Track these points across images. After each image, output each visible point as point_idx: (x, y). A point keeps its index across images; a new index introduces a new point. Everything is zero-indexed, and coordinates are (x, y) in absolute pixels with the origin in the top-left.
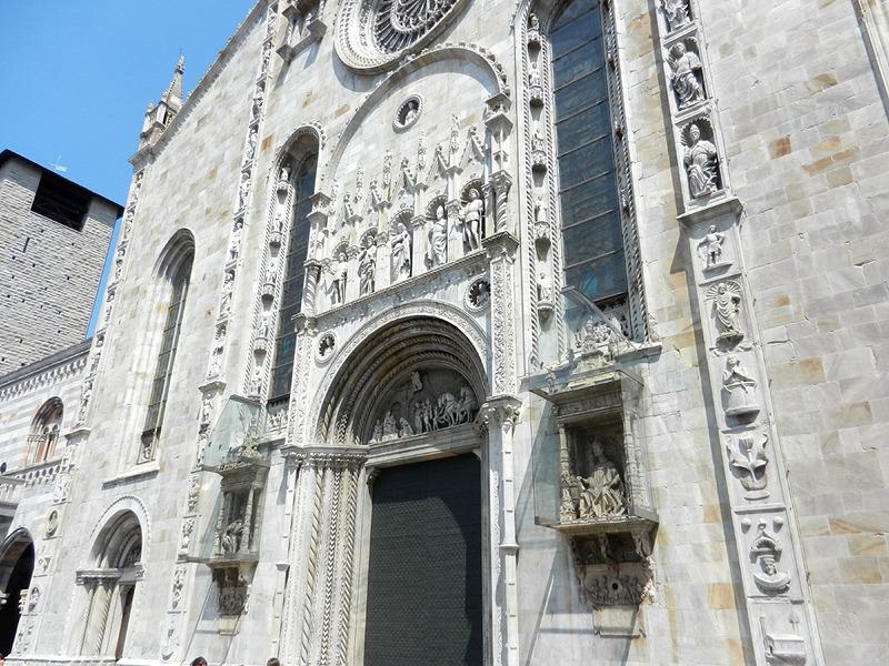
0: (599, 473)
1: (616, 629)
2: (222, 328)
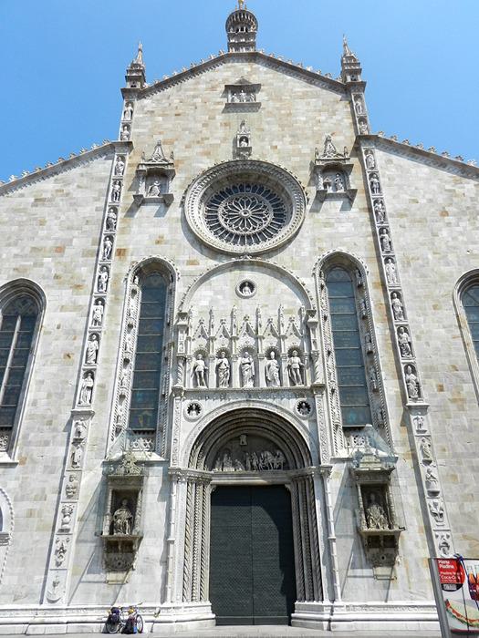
0: (375, 507)
1: (383, 576)
2: (90, 373)
